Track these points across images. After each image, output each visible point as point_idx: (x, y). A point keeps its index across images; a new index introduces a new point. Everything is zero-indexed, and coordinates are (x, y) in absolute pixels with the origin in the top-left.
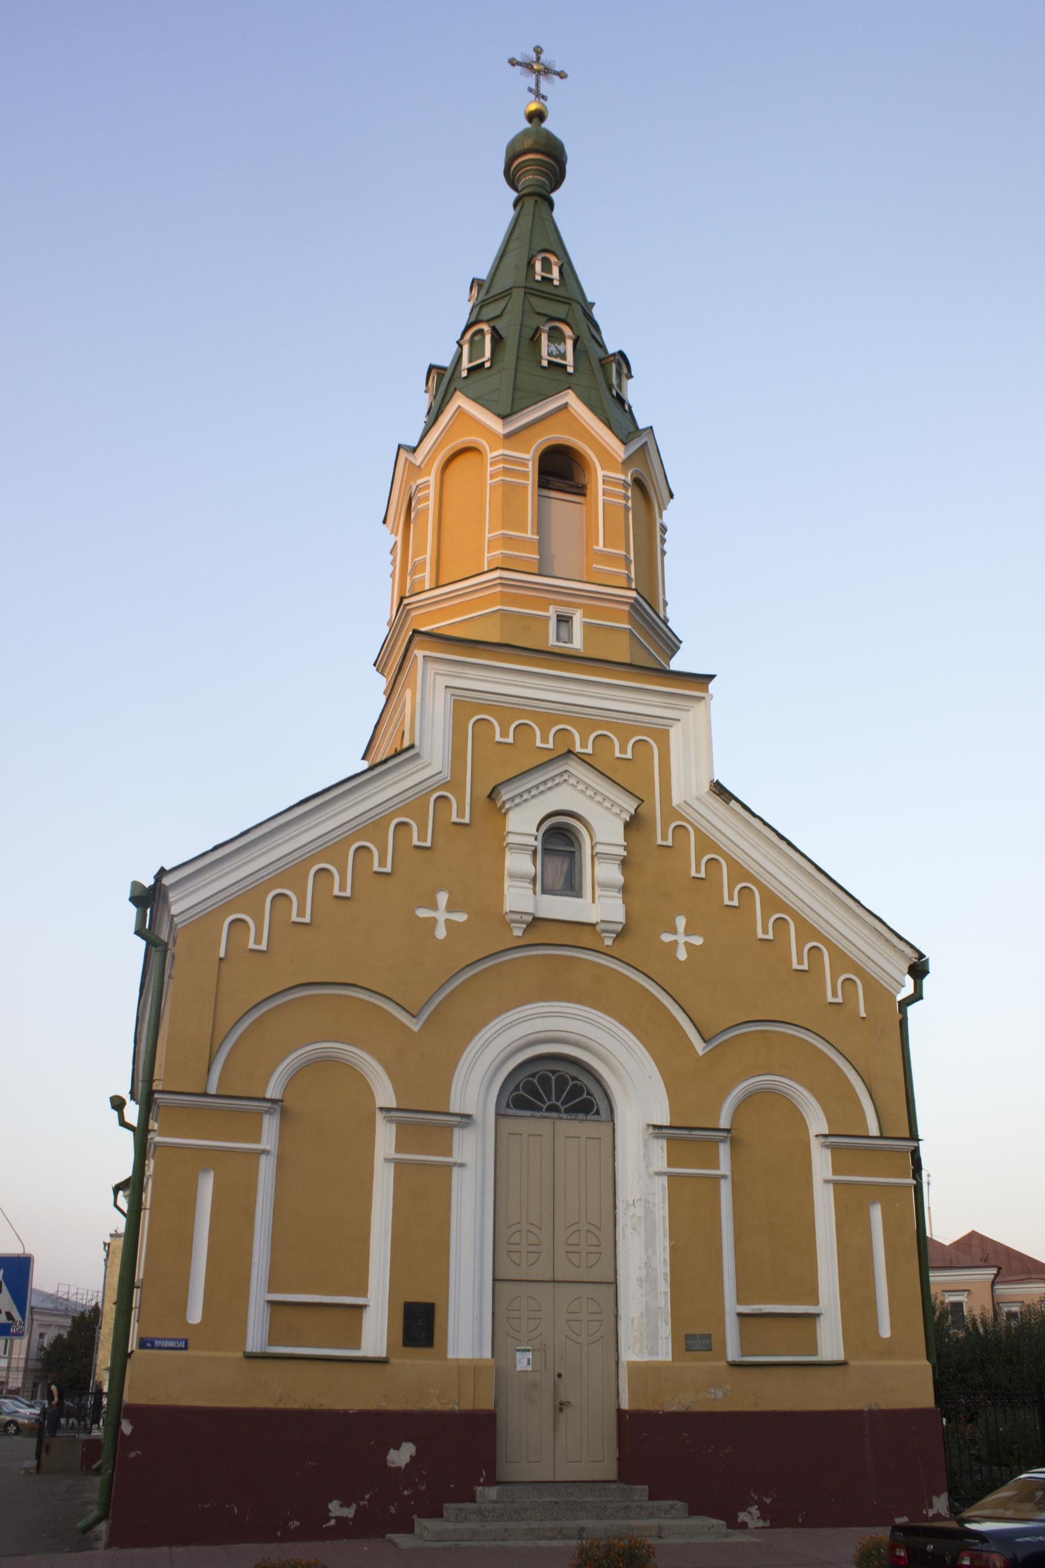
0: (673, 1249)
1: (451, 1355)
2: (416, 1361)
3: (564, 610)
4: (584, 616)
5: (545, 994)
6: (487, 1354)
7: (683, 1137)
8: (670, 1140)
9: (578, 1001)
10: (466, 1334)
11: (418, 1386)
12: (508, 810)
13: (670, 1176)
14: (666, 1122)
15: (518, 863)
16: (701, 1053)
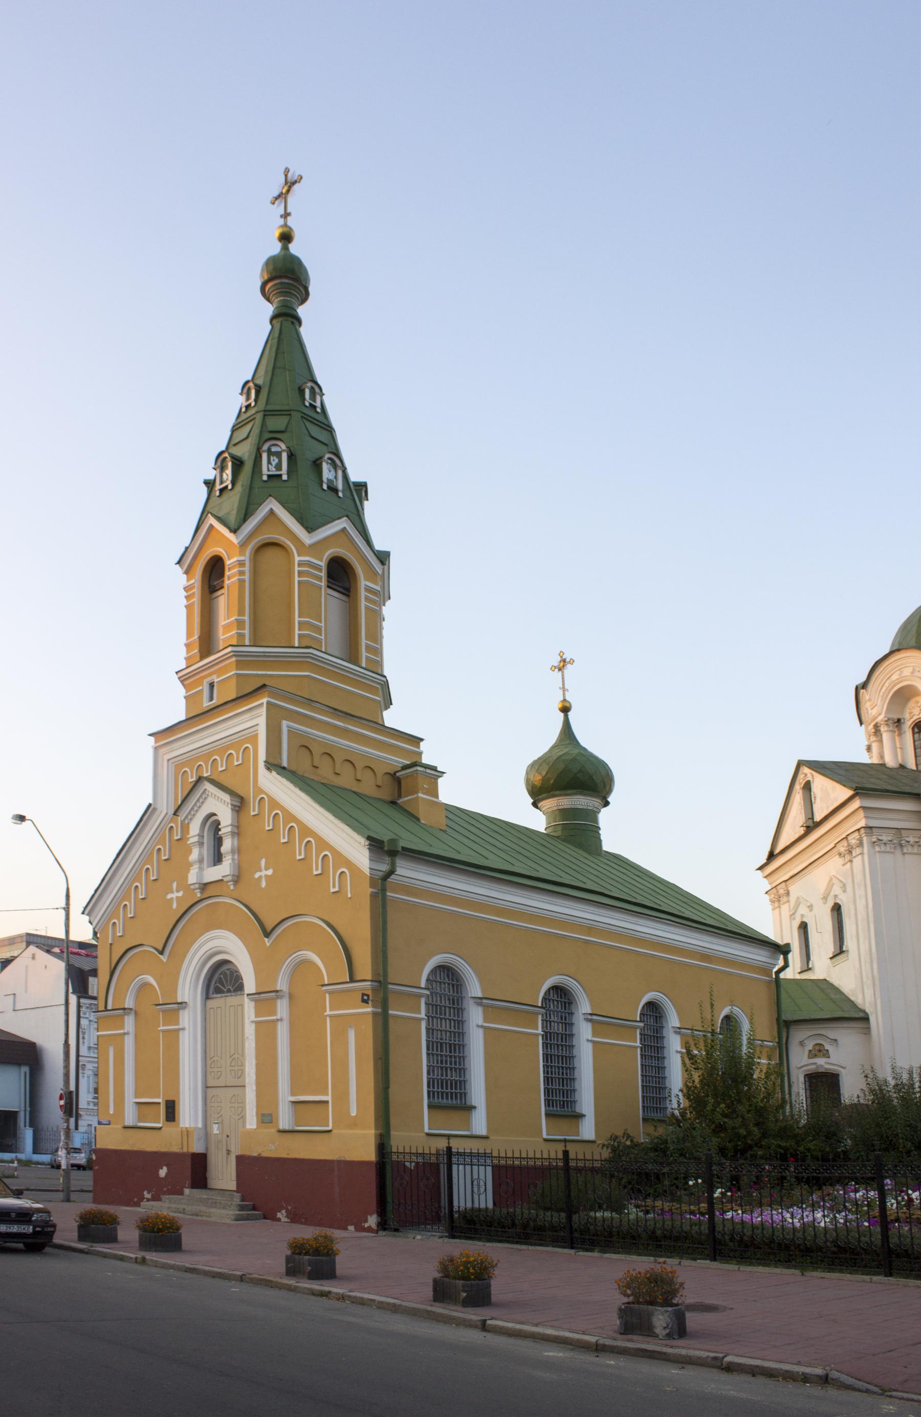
0: (257, 1065)
1: (181, 1126)
2: (169, 1130)
3: (209, 679)
4: (218, 677)
5: (208, 930)
6: (200, 1125)
7: (265, 998)
8: (256, 1001)
9: (220, 928)
10: (189, 1116)
11: (164, 1140)
12: (188, 824)
13: (256, 1023)
14: (254, 991)
15: (194, 855)
16: (268, 945)
